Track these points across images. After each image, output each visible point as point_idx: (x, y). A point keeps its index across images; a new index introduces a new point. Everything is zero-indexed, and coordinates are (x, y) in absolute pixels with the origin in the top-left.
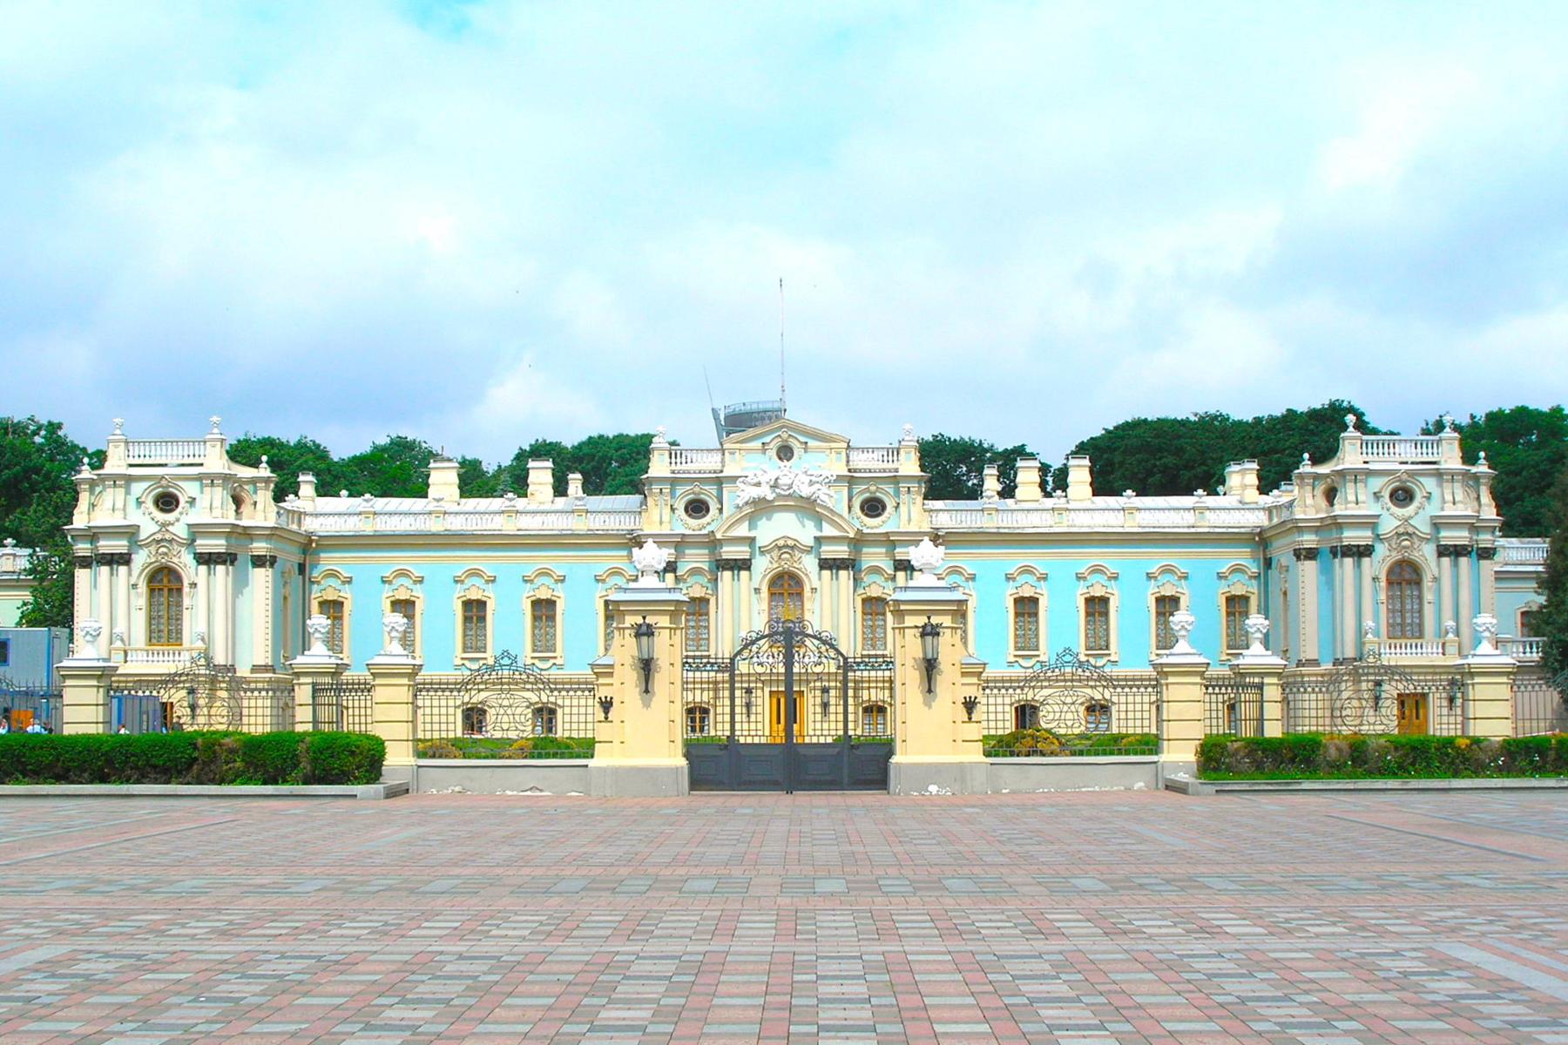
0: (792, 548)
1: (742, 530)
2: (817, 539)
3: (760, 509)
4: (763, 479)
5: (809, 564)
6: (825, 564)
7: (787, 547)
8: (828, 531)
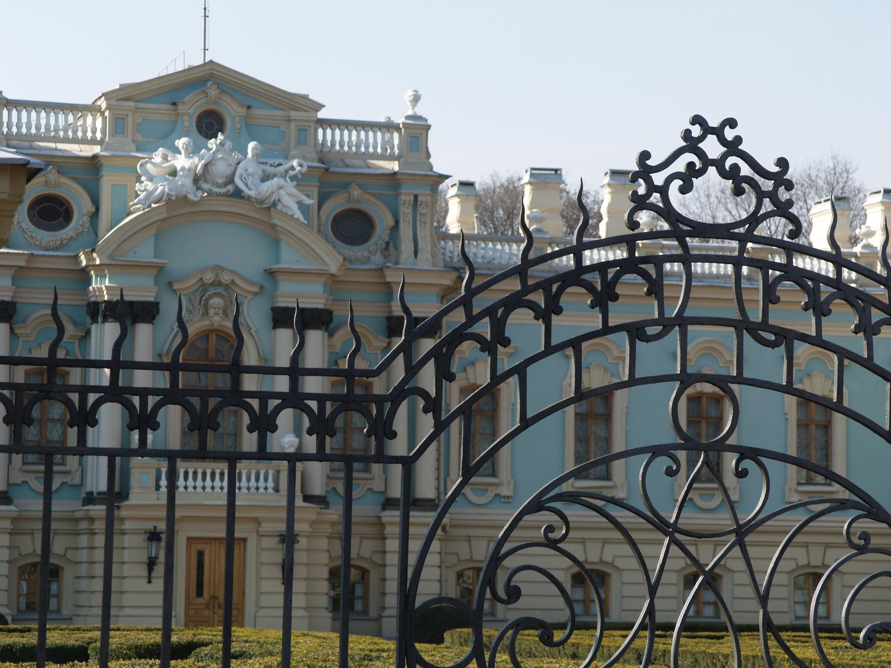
0: (227, 287)
1: (145, 253)
2: (271, 274)
3: (176, 212)
4: (181, 162)
5: (255, 316)
6: (281, 317)
7: (216, 285)
8: (289, 259)
